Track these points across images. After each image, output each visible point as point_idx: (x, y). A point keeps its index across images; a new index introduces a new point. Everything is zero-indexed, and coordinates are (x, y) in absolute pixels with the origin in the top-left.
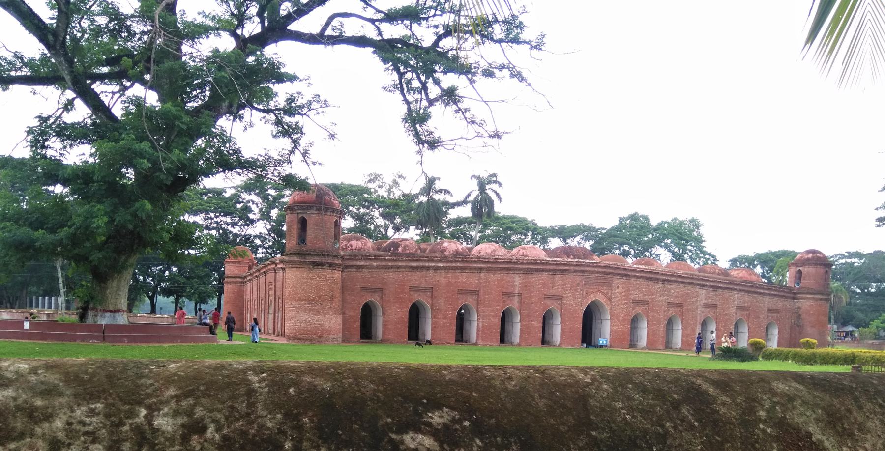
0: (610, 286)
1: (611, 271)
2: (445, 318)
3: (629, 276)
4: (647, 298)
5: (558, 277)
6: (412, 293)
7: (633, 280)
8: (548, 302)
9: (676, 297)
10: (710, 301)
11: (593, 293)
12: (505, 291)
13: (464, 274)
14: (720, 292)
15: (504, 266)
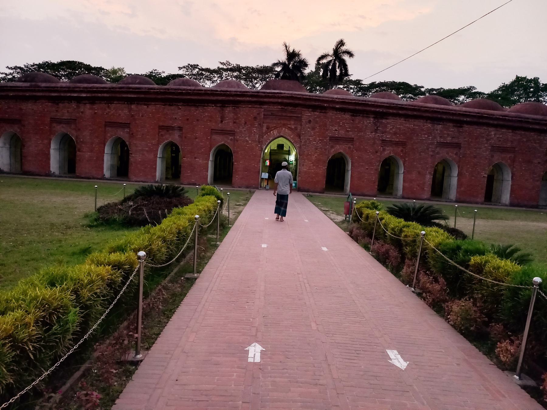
0: (298, 119)
1: (301, 102)
2: (91, 151)
3: (325, 108)
4: (351, 134)
5: (229, 111)
6: (54, 125)
7: (331, 114)
8: (215, 137)
9: (395, 134)
10: (449, 139)
11: (275, 128)
12: (161, 124)
13: (113, 106)
14: (466, 128)
15: (159, 97)
